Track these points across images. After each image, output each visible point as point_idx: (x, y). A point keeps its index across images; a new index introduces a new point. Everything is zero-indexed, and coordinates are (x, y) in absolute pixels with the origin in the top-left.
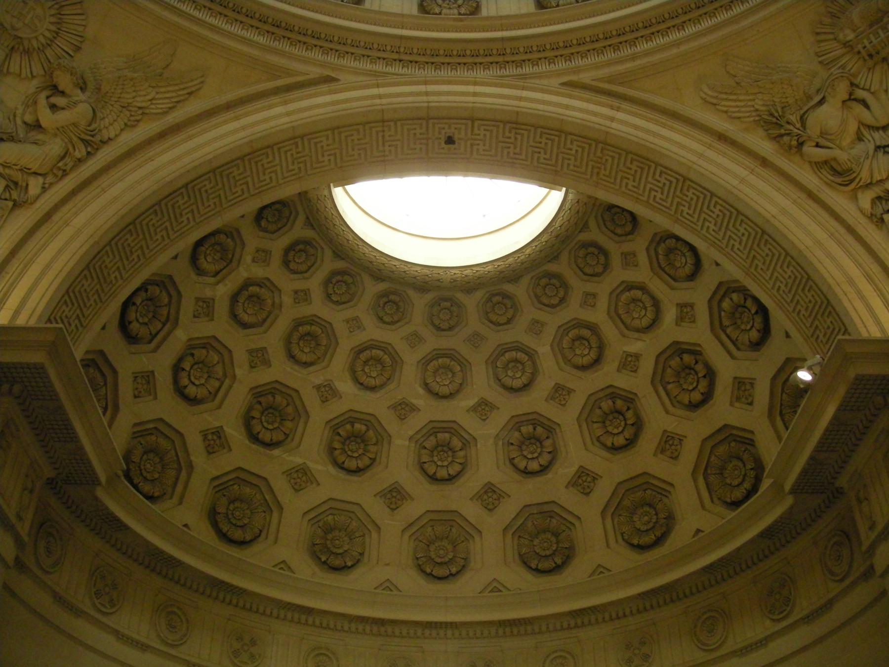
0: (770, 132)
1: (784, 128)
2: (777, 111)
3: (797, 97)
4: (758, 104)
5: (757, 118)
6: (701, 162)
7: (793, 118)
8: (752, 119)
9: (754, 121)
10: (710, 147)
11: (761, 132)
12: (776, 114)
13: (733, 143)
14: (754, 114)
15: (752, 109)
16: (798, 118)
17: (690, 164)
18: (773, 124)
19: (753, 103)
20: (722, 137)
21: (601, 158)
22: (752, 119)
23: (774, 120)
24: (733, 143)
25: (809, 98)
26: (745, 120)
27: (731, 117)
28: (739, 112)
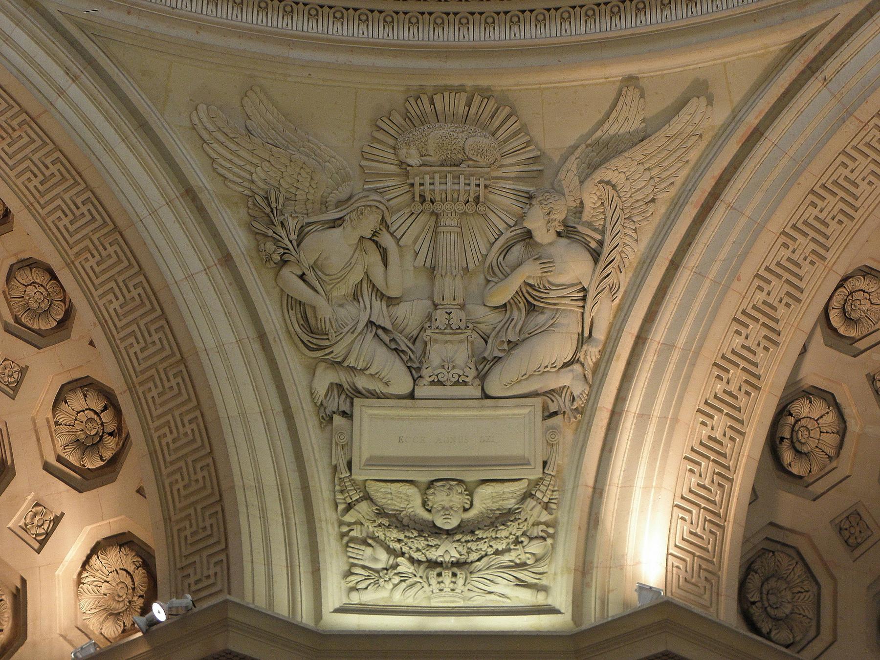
0: (254, 223)
1: (276, 228)
2: (277, 200)
3: (310, 197)
4: (259, 174)
5: (247, 192)
6: (149, 221)
7: (292, 224)
8: (241, 189)
9: (241, 193)
10: (169, 203)
11: (243, 211)
12: (274, 205)
13: (201, 211)
14: (246, 184)
15: (248, 176)
16: (298, 227)
17: (136, 219)
18: (266, 213)
19: (253, 170)
20: (190, 194)
21: (14, 130)
22: (241, 189)
23: (268, 210)
24: (201, 211)
25: (324, 205)
26: (231, 185)
27: (214, 169)
28: (228, 169)
